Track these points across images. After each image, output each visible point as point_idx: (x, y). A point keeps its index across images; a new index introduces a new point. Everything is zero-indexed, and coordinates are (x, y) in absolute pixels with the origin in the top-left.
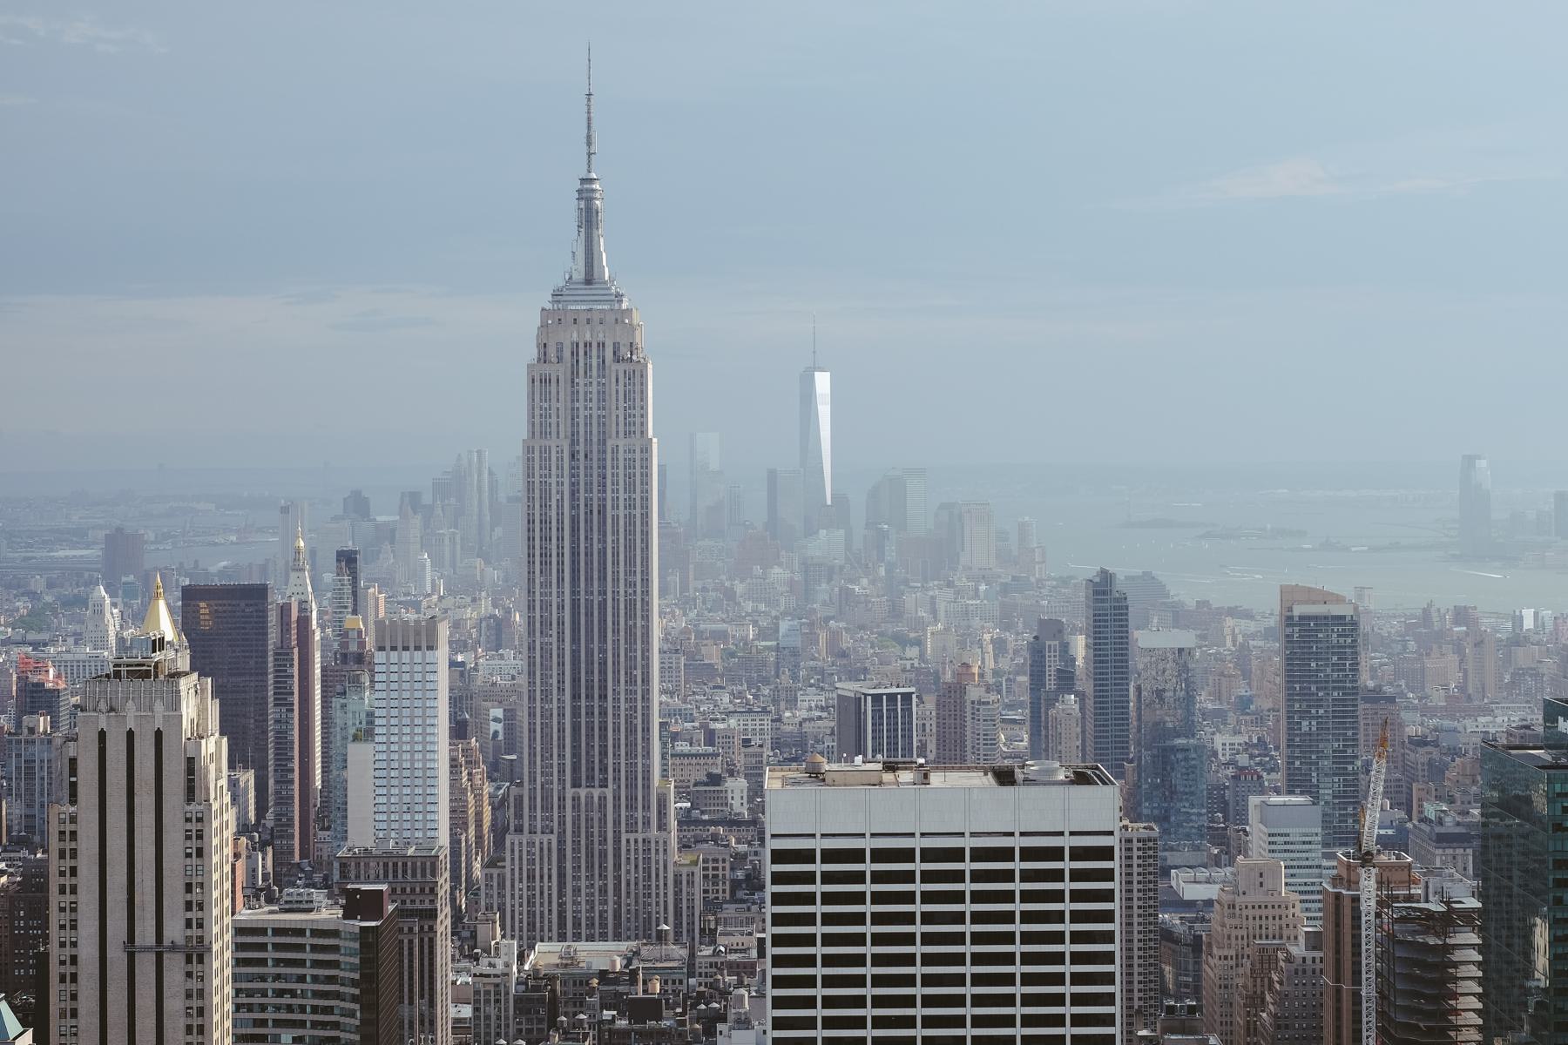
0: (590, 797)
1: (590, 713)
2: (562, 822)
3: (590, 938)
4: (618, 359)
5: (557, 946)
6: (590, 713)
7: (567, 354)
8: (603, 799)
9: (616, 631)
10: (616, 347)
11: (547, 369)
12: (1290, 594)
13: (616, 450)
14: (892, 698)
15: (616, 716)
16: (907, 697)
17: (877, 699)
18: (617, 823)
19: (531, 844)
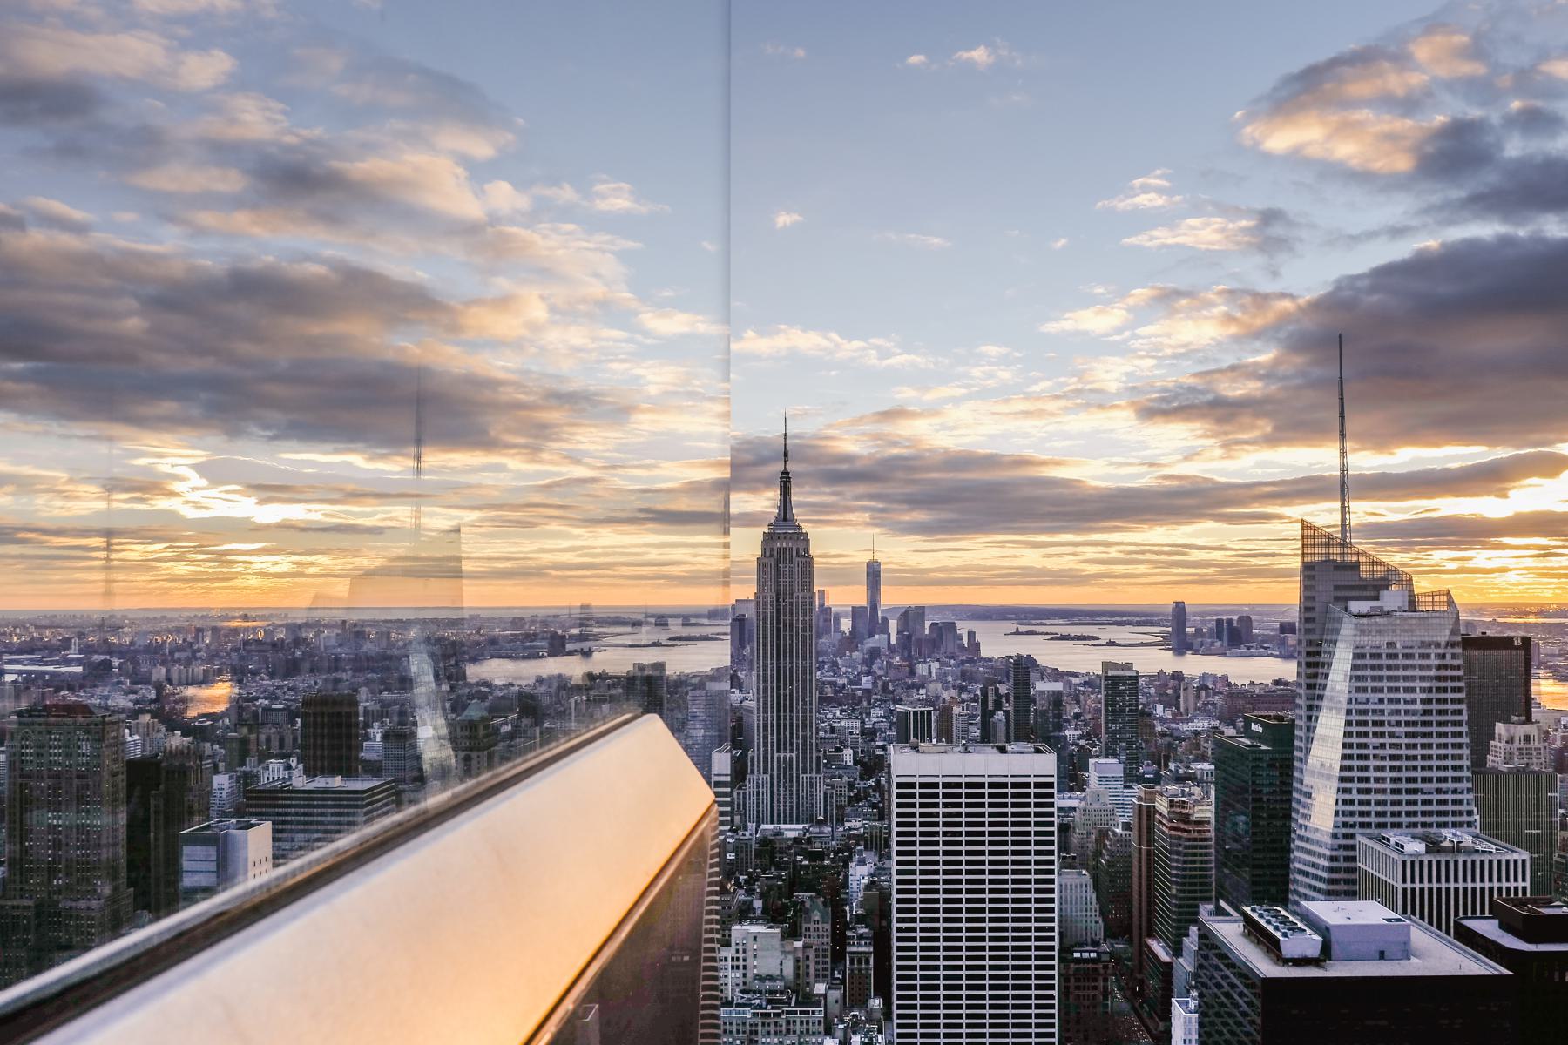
0: (785, 758)
1: (785, 719)
2: (772, 769)
3: (785, 823)
4: (798, 555)
5: (770, 827)
6: (785, 719)
7: (775, 553)
8: (791, 758)
9: (797, 681)
10: (798, 550)
11: (766, 560)
12: (1107, 665)
13: (797, 597)
14: (922, 712)
15: (798, 720)
16: (929, 712)
17: (916, 713)
18: (798, 769)
19: (758, 779)
